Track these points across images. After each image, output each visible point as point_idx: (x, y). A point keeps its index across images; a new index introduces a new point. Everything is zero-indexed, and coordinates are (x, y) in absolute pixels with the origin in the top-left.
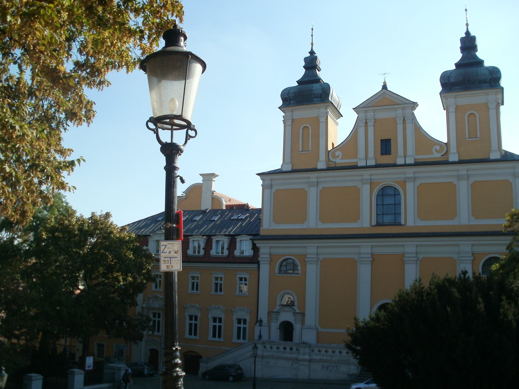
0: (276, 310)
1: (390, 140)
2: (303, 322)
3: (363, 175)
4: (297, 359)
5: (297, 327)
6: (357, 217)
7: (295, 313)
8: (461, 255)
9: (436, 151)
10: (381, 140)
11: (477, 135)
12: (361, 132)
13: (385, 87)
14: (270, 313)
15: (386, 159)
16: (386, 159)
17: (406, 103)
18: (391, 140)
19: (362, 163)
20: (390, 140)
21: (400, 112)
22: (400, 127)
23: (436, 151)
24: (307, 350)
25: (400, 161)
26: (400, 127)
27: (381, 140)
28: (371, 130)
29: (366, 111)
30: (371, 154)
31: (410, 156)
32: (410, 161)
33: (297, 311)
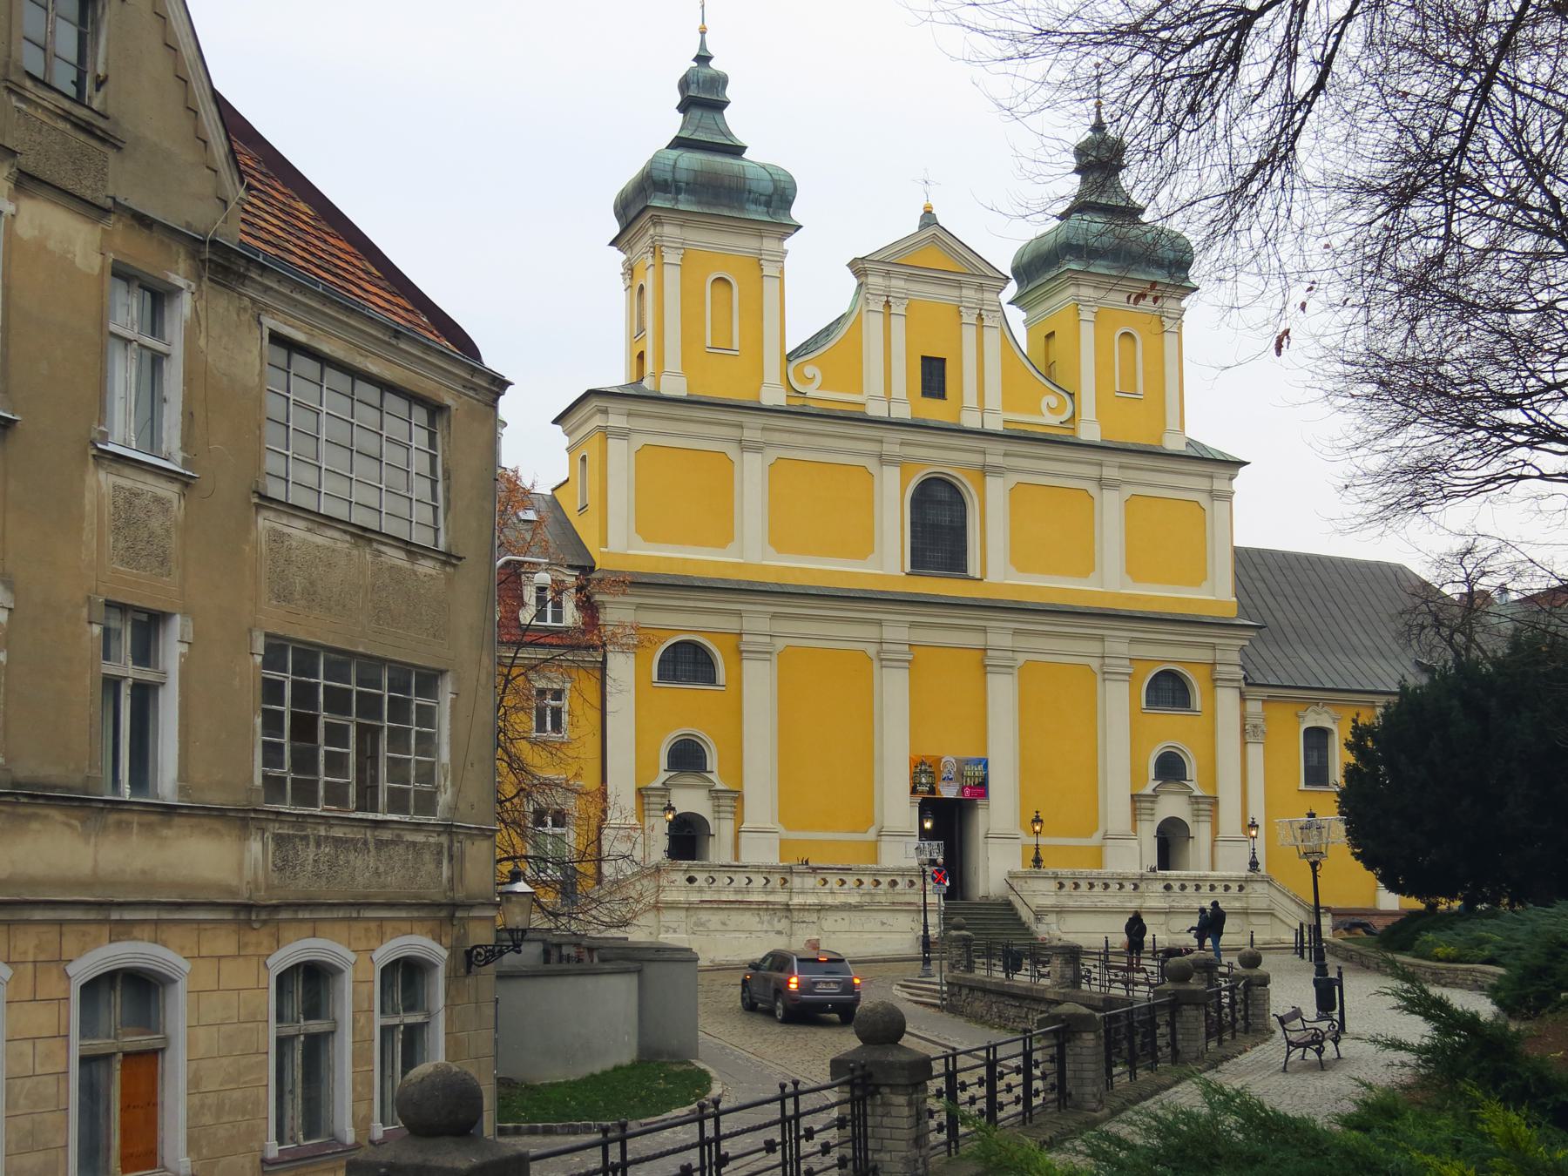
0: (658, 784)
1: (943, 360)
2: (738, 815)
3: (882, 442)
4: (787, 908)
5: (722, 830)
6: (864, 545)
7: (715, 794)
8: (1107, 661)
9: (1050, 409)
10: (924, 358)
11: (1135, 385)
12: (874, 324)
13: (928, 218)
14: (642, 793)
15: (934, 411)
16: (934, 411)
17: (988, 276)
18: (947, 362)
19: (876, 410)
20: (943, 360)
21: (968, 293)
22: (969, 334)
23: (1050, 409)
24: (811, 881)
25: (970, 421)
26: (969, 334)
27: (924, 358)
28: (898, 325)
29: (888, 273)
30: (899, 388)
31: (994, 411)
32: (994, 424)
33: (719, 786)
